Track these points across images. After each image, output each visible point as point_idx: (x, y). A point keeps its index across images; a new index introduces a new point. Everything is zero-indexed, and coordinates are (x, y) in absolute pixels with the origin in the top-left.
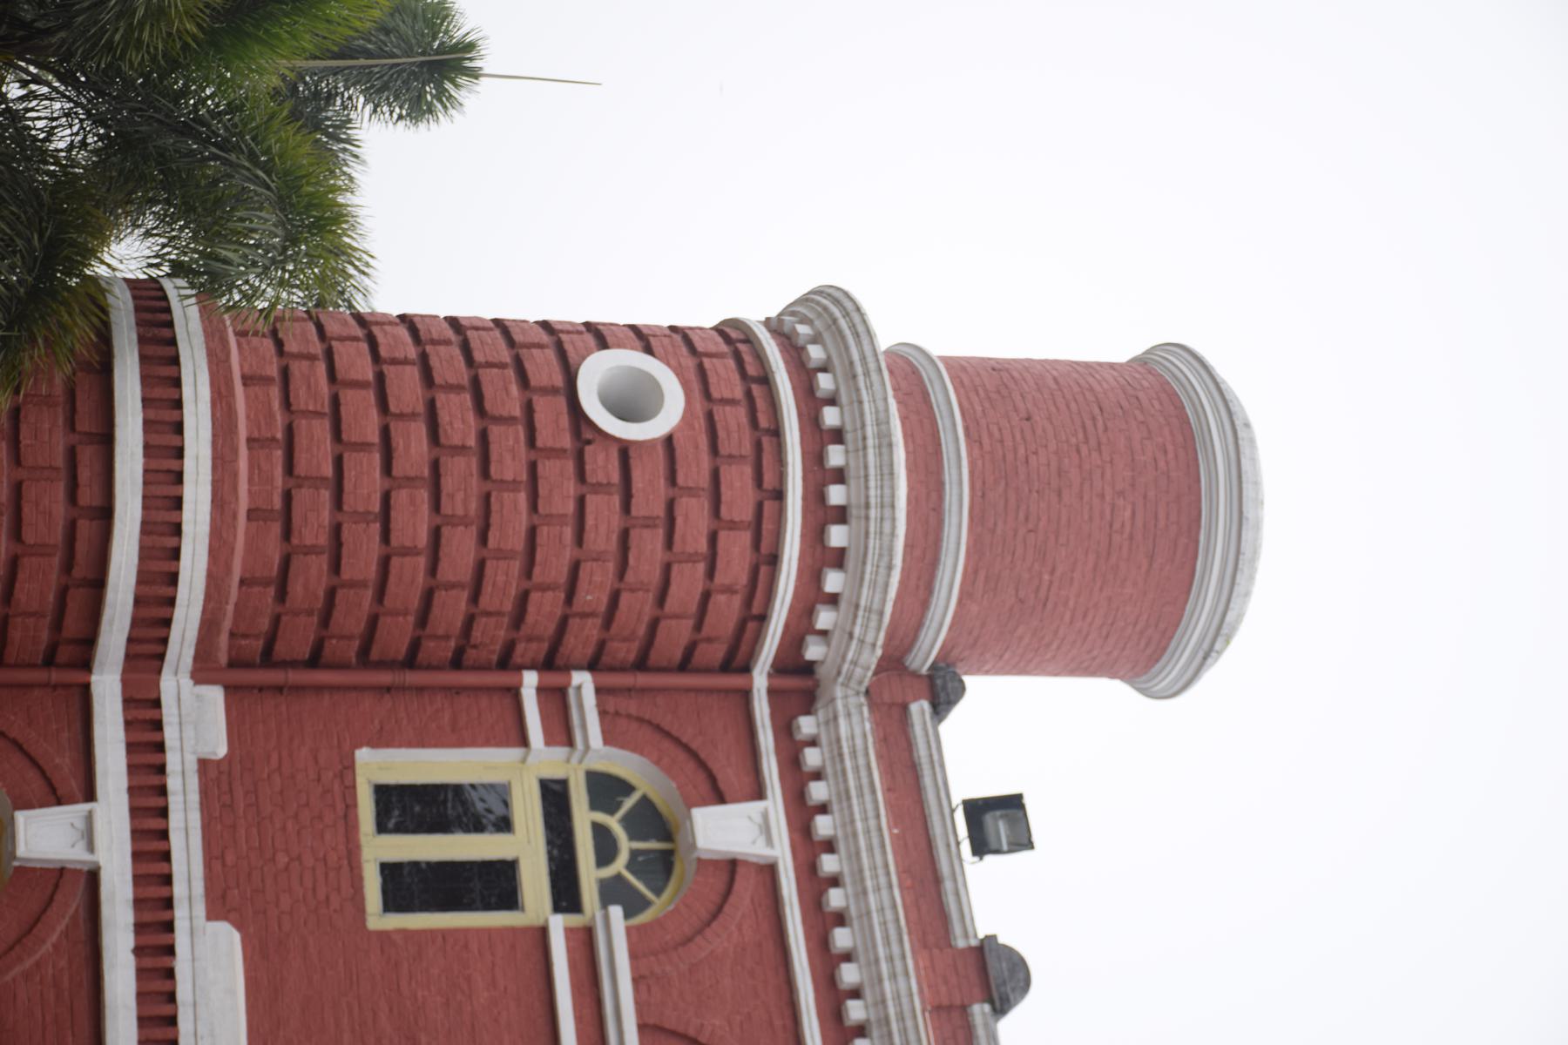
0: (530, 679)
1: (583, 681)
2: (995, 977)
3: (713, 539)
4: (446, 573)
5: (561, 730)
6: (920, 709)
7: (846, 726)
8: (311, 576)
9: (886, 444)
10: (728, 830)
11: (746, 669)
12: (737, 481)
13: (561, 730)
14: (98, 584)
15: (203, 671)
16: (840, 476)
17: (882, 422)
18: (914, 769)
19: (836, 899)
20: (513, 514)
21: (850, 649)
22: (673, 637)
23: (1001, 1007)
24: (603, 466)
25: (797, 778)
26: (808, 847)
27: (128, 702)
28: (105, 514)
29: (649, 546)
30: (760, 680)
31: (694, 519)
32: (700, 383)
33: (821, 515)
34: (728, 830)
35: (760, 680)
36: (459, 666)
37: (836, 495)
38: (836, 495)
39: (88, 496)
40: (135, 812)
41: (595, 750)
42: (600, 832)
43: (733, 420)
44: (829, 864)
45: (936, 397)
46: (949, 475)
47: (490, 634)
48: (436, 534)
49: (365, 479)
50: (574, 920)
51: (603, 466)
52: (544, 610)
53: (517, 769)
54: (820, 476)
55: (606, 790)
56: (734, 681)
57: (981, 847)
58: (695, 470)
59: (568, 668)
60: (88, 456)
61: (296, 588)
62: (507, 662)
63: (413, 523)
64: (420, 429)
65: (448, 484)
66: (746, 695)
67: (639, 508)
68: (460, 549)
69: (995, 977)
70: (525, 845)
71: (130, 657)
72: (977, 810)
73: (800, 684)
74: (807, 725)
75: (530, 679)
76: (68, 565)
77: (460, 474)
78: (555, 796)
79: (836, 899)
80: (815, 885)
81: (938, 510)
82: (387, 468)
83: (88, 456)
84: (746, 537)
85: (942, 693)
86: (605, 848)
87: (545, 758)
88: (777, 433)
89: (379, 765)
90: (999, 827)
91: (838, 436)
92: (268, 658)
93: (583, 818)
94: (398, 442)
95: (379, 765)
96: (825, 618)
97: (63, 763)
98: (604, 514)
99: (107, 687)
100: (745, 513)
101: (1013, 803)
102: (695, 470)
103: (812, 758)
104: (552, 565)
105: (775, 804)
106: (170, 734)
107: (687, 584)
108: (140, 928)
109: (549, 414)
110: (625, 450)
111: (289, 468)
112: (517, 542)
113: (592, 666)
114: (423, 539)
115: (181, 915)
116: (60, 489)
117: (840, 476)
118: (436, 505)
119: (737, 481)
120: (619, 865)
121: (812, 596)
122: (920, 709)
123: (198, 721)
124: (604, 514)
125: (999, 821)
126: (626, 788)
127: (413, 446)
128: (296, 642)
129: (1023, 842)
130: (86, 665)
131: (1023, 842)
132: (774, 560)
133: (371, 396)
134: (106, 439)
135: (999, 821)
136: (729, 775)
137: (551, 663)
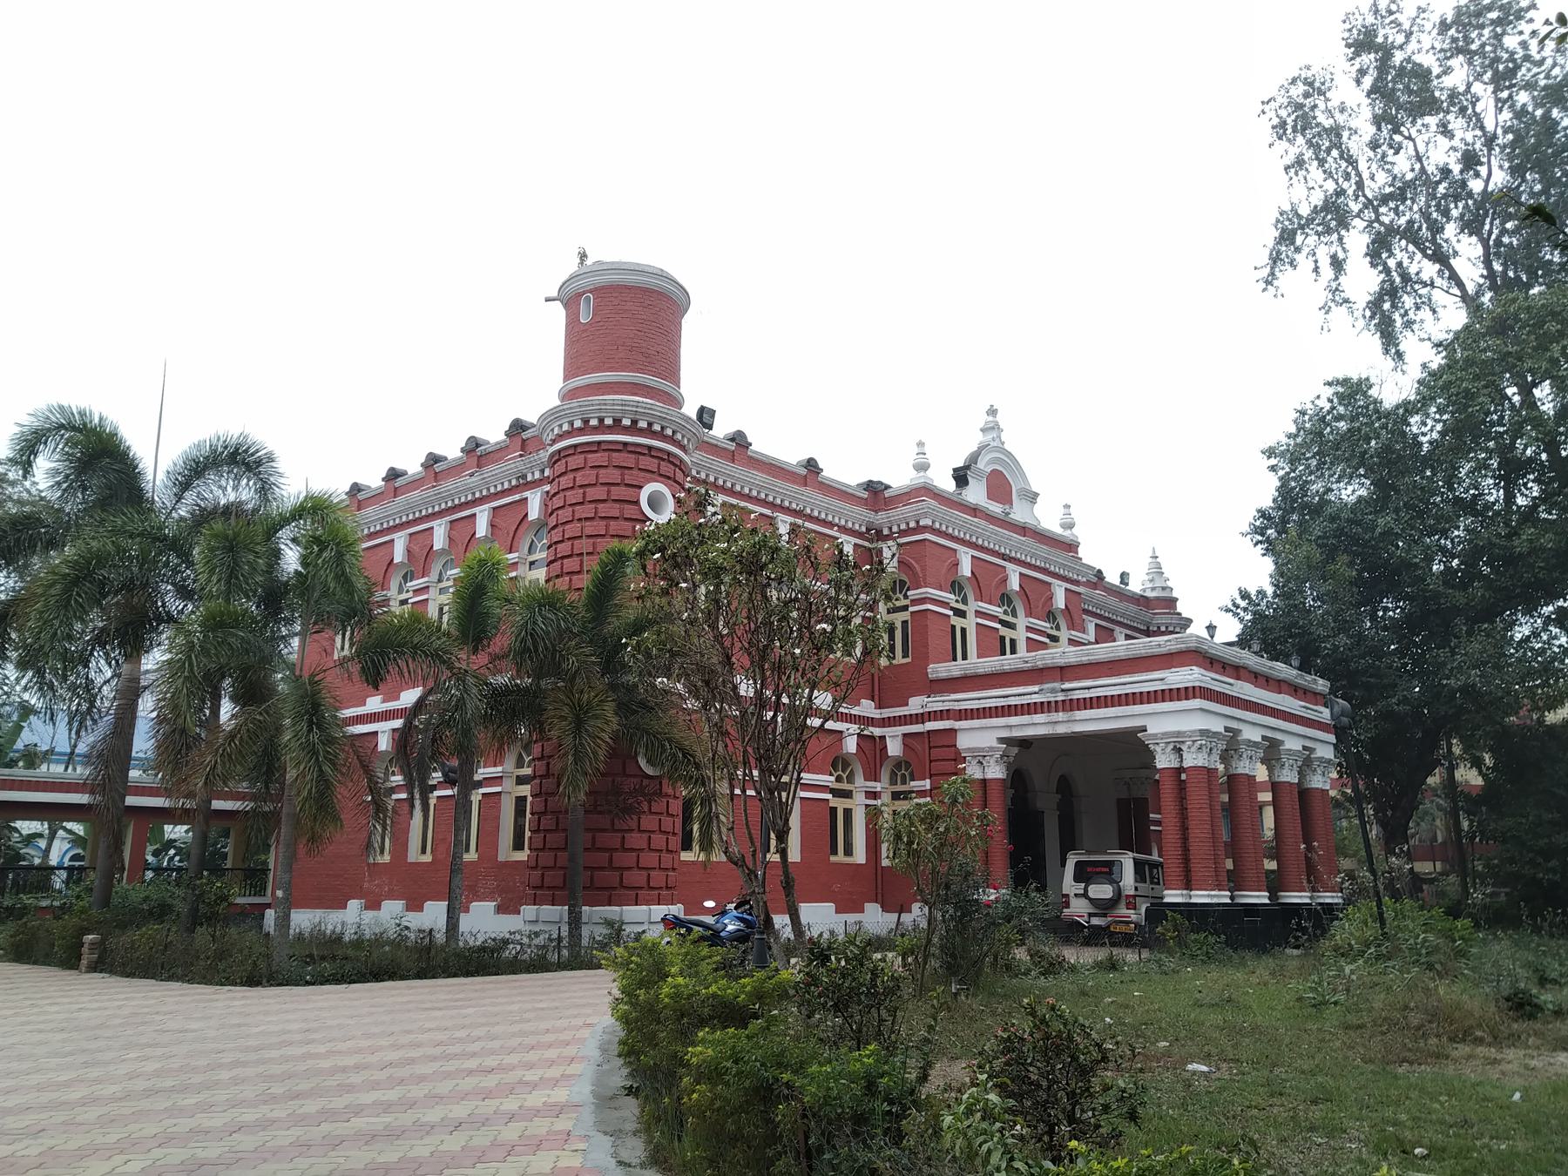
2: (739, 439)
45: (652, 384)
57: (710, 428)
69: (739, 439)
129: (712, 413)
131: (712, 413)
135: (706, 416)
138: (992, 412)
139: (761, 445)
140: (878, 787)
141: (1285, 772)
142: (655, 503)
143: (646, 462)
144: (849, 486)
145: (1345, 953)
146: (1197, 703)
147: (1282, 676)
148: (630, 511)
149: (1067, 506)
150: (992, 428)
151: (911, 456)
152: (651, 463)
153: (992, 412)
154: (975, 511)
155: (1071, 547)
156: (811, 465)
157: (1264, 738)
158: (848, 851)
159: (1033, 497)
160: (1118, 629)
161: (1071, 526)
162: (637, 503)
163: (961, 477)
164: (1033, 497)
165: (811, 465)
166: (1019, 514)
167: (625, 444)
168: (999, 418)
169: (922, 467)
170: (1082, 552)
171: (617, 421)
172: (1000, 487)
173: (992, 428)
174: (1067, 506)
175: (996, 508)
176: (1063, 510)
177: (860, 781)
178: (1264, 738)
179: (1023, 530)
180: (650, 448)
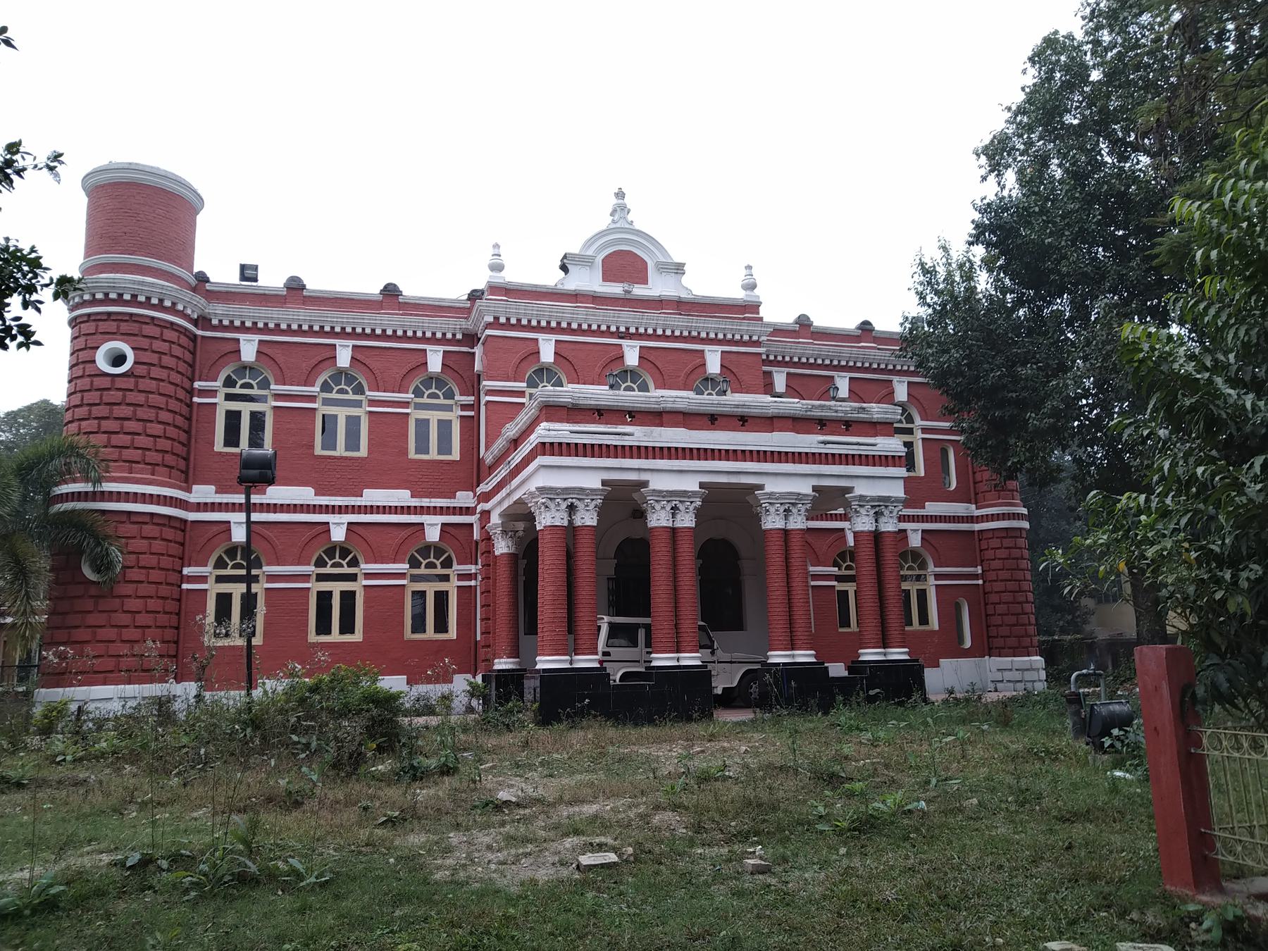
0: (196, 399)
1: (197, 384)
2: (295, 287)
3: (165, 341)
4: (170, 421)
5: (213, 393)
6: (208, 286)
7: (218, 311)
8: (170, 459)
9: (142, 283)
10: (249, 351)
11: (195, 336)
12: (148, 330)
13: (213, 393)
14: (170, 517)
15: (189, 490)
16: (148, 299)
17: (134, 282)
18: (227, 292)
19: (271, 325)
20: (155, 399)
21: (195, 304)
22: (188, 357)
23: (303, 287)
24: (142, 370)
25: (231, 328)
26: (254, 329)
27: (198, 510)
28: (152, 515)
29: (167, 360)
30: (200, 333)
31: (158, 345)
32: (111, 335)
33: (160, 307)
34: (249, 351)
35: (200, 333)
36: (192, 420)
37: (155, 301)
38: (155, 301)
39: (147, 519)
40: (234, 511)
41: (218, 383)
42: (243, 386)
43: (125, 327)
44: (261, 325)
46: (146, 264)
47: (185, 410)
48: (160, 423)
49: (142, 441)
50: (270, 398)
51: (142, 370)
52: (181, 394)
53: (223, 406)
54: (147, 304)
55: (229, 382)
56: (199, 340)
57: (256, 280)
58: (145, 343)
59: (193, 389)
60: (134, 519)
61: (173, 464)
62: (190, 405)
63: (156, 429)
64: (126, 423)
65: (145, 417)
66: (203, 337)
67: (155, 361)
68: (165, 416)
69: (295, 287)
70: (246, 408)
71: (186, 510)
72: (243, 277)
73: (203, 321)
74: (215, 322)
75: (196, 399)
76: (164, 525)
77: (141, 413)
78: (229, 397)
79: (271, 325)
80: (266, 330)
81: (157, 269)
82: (139, 434)
83: (134, 519)
84: (165, 331)
85: (202, 278)
86: (249, 386)
87: (219, 399)
88: (131, 315)
89: (219, 446)
90: (248, 273)
91: (134, 296)
92: (186, 472)
93: (237, 390)
94: (131, 430)
95: (219, 446)
96: (189, 311)
97: (215, 529)
98: (156, 372)
99: (192, 516)
100: (158, 330)
101: (243, 267)
102: (145, 343)
103: (226, 323)
104: (170, 389)
105: (242, 337)
106: (209, 501)
107: (177, 351)
108: (268, 512)
109: (120, 383)
110: (135, 363)
111: (138, 462)
112: (164, 399)
113: (192, 380)
114: (161, 426)
115: (265, 501)
116: (144, 527)
117: (148, 299)
118: (151, 421)
119: (148, 330)
120: (254, 383)
121: (182, 314)
122: (208, 286)
123: (203, 492)
124: (156, 372)
125: (248, 272)
126: (229, 377)
127: (131, 426)
128: (182, 464)
129: (256, 268)
130: (186, 521)
131: (256, 268)
132: (172, 323)
133: (113, 436)
134: (129, 513)
135: (248, 272)
136: (230, 347)
137: (191, 392)
138: (620, 195)
139: (314, 284)
140: (472, 569)
141: (769, 518)
142: (119, 360)
143: (103, 326)
144: (458, 301)
145: (109, 730)
146: (541, 460)
147: (771, 412)
148: (89, 369)
149: (749, 267)
150: (620, 210)
151: (487, 258)
152: (111, 326)
153: (620, 195)
154: (575, 297)
155: (751, 308)
156: (391, 292)
157: (702, 485)
158: (441, 626)
159: (679, 269)
160: (895, 379)
161: (752, 287)
162: (94, 361)
163: (564, 268)
164: (679, 269)
165: (391, 292)
166: (657, 287)
167: (89, 315)
168: (626, 200)
169: (496, 268)
170: (763, 312)
171: (134, 296)
172: (625, 264)
173: (620, 210)
174: (749, 267)
175: (616, 289)
176: (745, 272)
177: (455, 566)
178: (702, 485)
179: (659, 303)
180: (109, 314)
